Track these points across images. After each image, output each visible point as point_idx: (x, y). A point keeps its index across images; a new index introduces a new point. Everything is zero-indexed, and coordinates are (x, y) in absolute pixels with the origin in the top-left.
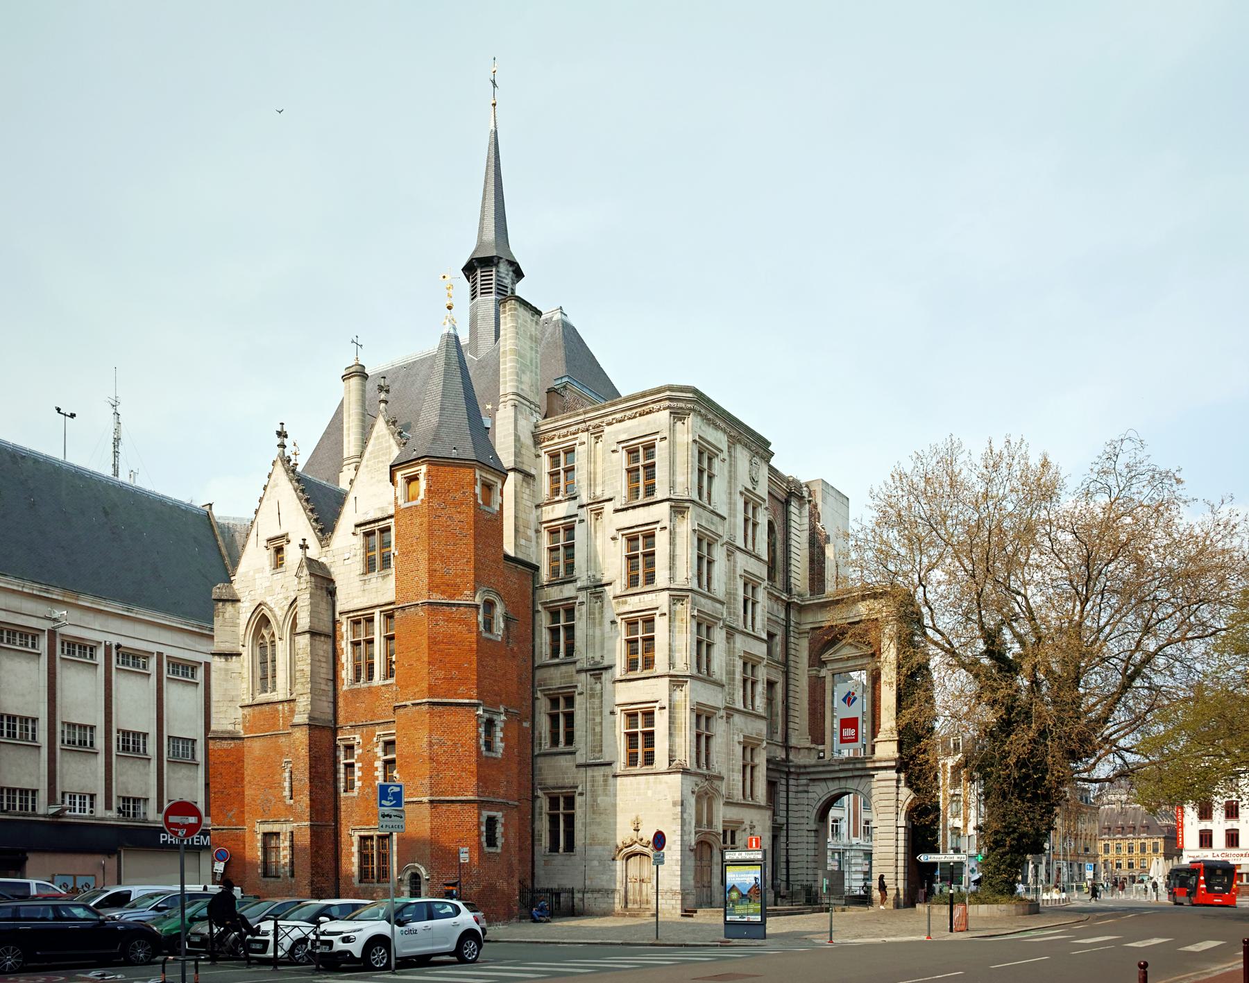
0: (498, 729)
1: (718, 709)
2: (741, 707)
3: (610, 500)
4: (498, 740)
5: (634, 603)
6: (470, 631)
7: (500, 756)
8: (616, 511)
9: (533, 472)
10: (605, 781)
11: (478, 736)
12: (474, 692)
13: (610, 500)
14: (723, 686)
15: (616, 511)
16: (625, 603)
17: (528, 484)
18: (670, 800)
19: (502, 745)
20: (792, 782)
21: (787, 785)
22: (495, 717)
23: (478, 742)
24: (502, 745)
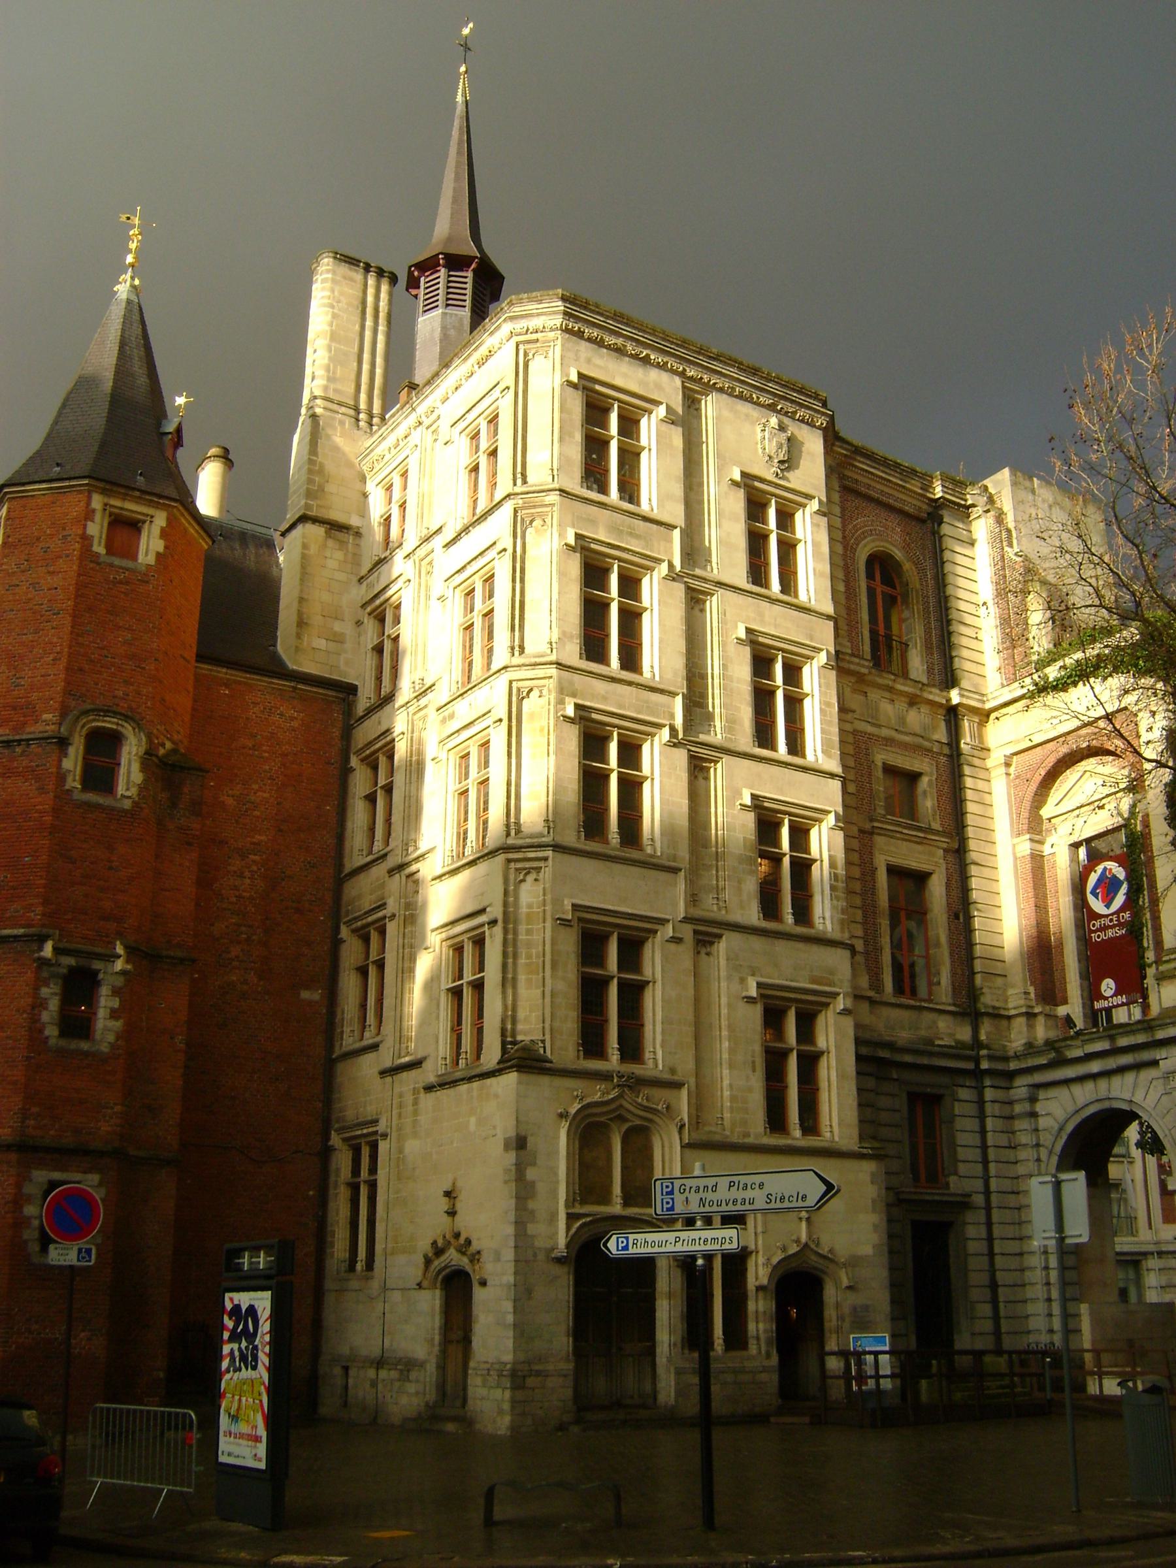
0: (104, 991)
1: (663, 922)
2: (752, 915)
3: (439, 530)
4: (102, 1013)
5: (464, 711)
6: (42, 790)
7: (105, 1048)
8: (448, 545)
9: (354, 521)
10: (416, 1102)
11: (42, 1004)
12: (36, 915)
13: (439, 530)
14: (675, 870)
15: (448, 545)
16: (452, 716)
17: (342, 544)
18: (500, 1138)
19: (118, 1024)
20: (989, 1094)
21: (981, 1102)
22: (97, 965)
23: (35, 1020)
24: (118, 1024)
